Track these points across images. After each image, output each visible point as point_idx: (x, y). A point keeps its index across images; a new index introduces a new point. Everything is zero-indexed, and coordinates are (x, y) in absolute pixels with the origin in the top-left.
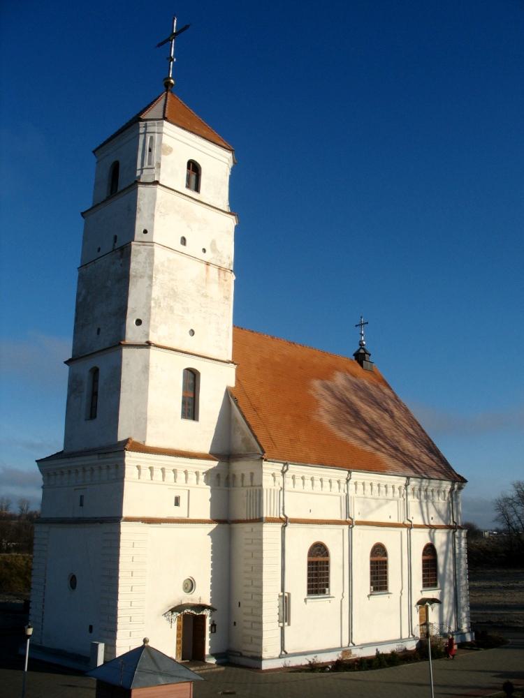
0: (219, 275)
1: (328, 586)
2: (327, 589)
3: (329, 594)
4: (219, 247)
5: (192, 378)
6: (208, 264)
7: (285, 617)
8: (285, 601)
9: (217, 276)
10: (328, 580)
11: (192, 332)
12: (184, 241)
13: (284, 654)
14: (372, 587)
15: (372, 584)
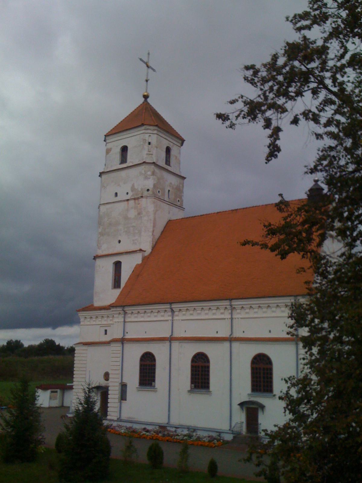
0: (135, 203)
1: (154, 381)
2: (153, 383)
3: (154, 386)
4: (136, 187)
5: (118, 265)
6: (128, 200)
7: (123, 396)
8: (124, 387)
9: (134, 204)
10: (154, 377)
11: (120, 242)
12: (116, 194)
13: (119, 420)
14: (193, 385)
15: (192, 382)
